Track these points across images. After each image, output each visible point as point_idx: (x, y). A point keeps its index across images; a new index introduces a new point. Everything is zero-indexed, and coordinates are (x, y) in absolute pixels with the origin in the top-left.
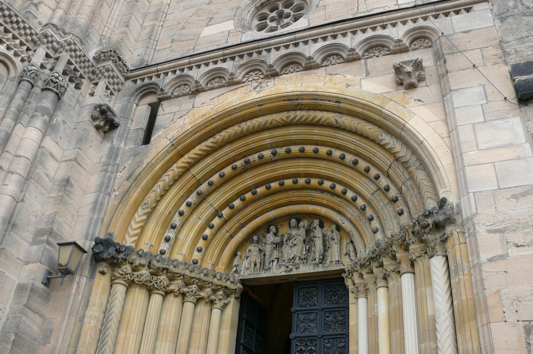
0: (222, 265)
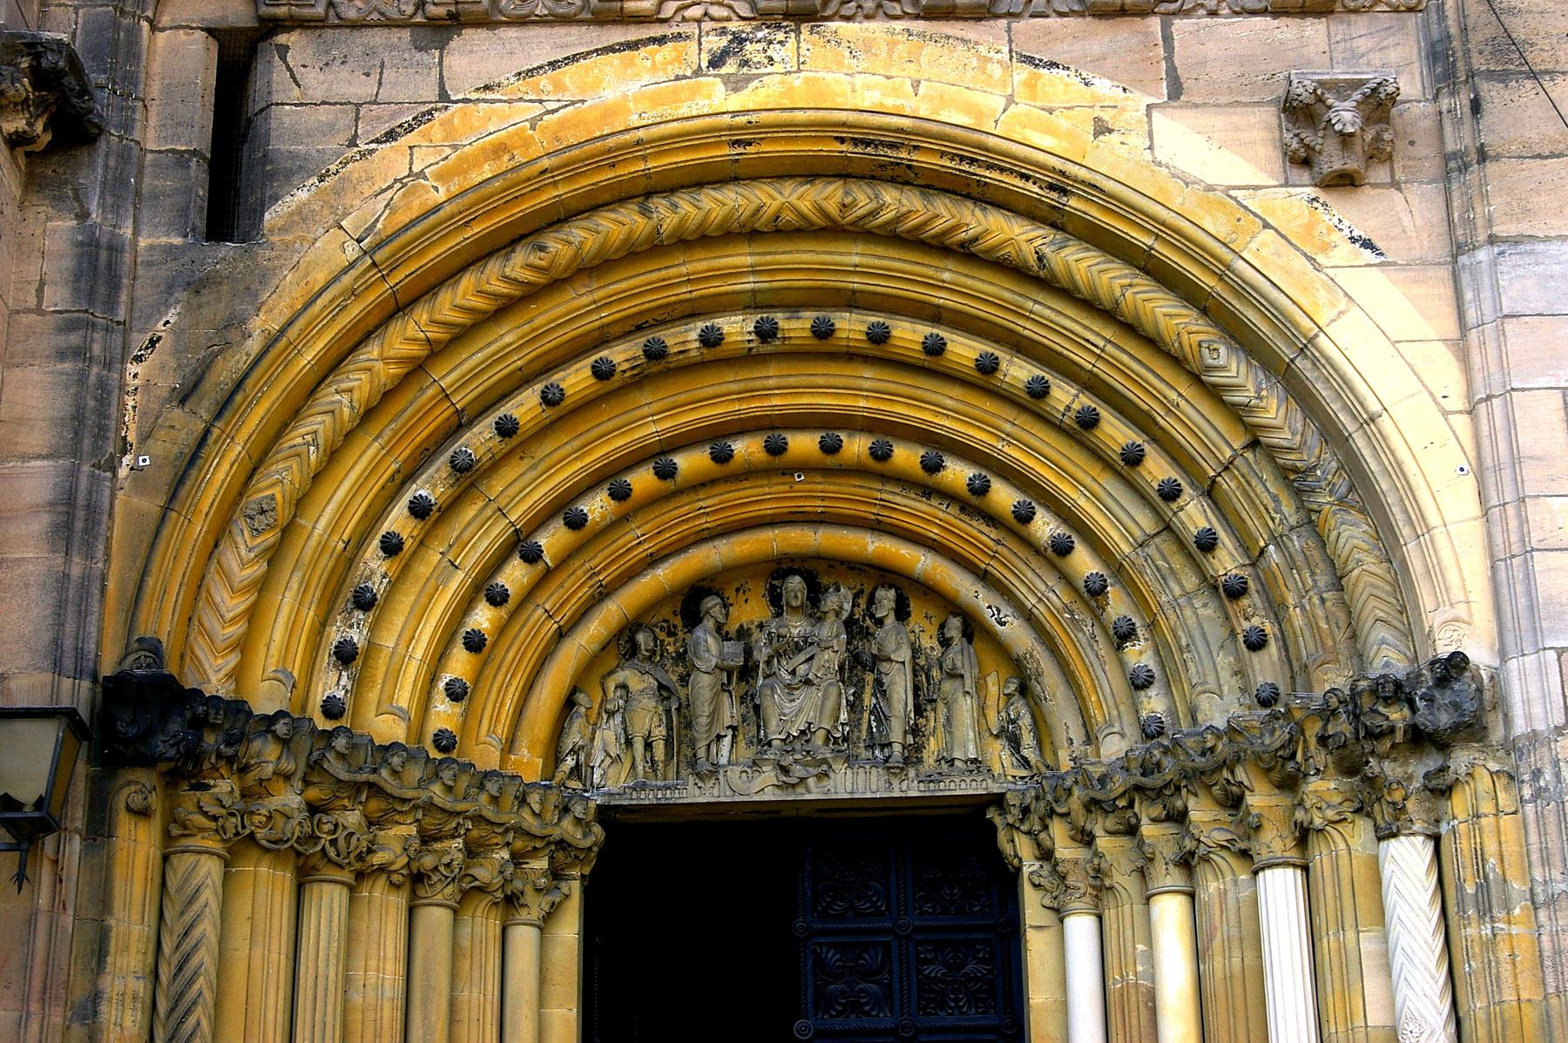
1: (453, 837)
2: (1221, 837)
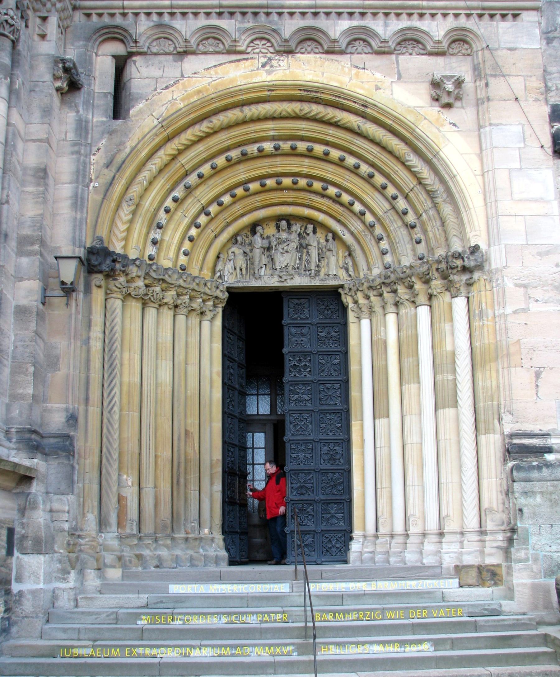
0: (207, 270)
1: (186, 295)
2: (407, 297)
